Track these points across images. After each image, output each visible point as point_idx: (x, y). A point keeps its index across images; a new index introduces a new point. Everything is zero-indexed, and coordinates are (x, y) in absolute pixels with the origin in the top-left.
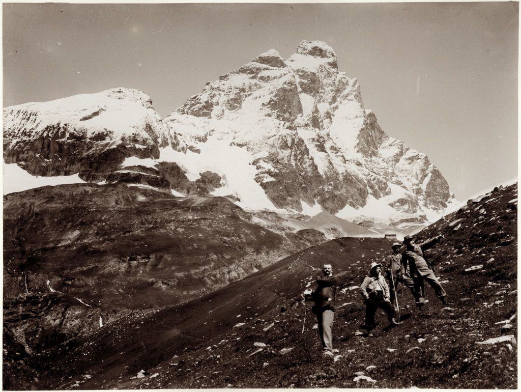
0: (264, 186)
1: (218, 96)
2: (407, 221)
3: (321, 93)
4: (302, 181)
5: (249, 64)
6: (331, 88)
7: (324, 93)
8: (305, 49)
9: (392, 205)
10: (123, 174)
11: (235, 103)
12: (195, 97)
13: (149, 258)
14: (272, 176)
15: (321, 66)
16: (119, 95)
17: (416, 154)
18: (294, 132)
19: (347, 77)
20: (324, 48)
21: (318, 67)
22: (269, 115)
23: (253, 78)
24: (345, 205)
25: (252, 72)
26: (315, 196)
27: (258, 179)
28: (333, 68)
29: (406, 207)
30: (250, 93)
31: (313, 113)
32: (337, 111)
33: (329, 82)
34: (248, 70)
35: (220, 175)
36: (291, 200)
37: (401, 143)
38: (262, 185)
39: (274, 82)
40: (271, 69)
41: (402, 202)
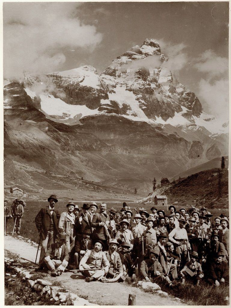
0: (143, 110)
2: (192, 125)
4: (155, 107)
8: (147, 43)
14: (145, 106)
15: (154, 51)
16: (86, 69)
17: (190, 92)
18: (150, 87)
20: (156, 42)
21: (153, 52)
22: (139, 78)
23: (129, 58)
25: (129, 56)
26: (159, 114)
27: (140, 107)
28: (159, 52)
38: (142, 109)
40: (137, 55)
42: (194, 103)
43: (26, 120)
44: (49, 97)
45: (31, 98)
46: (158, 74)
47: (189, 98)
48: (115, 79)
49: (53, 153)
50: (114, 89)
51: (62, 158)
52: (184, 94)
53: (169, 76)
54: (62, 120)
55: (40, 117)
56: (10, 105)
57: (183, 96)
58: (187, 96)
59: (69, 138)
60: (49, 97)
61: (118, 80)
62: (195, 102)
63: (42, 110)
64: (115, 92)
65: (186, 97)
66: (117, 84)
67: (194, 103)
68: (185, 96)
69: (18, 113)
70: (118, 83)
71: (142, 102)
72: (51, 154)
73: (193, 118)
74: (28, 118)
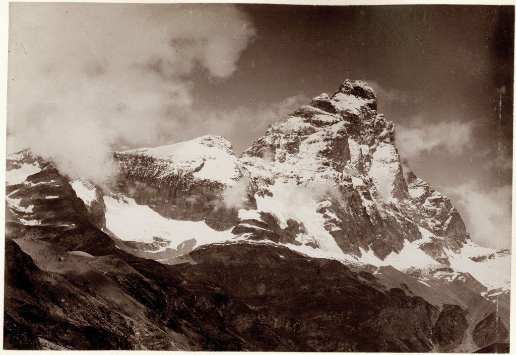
1: (279, 139)
2: (441, 270)
3: (362, 134)
4: (359, 230)
5: (304, 107)
6: (370, 130)
7: (364, 135)
8: (347, 88)
10: (246, 227)
11: (292, 148)
12: (261, 140)
13: (341, 313)
14: (337, 225)
15: (362, 107)
16: (210, 143)
17: (440, 197)
18: (350, 184)
19: (384, 119)
20: (366, 88)
22: (327, 164)
23: (307, 121)
25: (306, 116)
26: (369, 243)
27: (327, 228)
30: (305, 136)
31: (359, 160)
32: (375, 153)
33: (369, 123)
34: (303, 113)
35: (299, 222)
36: (353, 247)
37: (428, 185)
38: (331, 233)
39: (327, 128)
40: (323, 114)
42: (448, 221)
43: (71, 250)
44: (125, 202)
45: (86, 203)
46: (369, 158)
47: (438, 209)
49: (128, 324)
50: (271, 188)
51: (147, 335)
52: (427, 202)
53: (392, 161)
54: (153, 252)
55: (102, 243)
56: (38, 218)
57: (424, 205)
58: (433, 205)
59: (165, 291)
60: (125, 202)
61: (279, 167)
62: (450, 218)
63: (107, 230)
64: (271, 195)
65: (430, 208)
66: (277, 176)
67: (448, 221)
68: (429, 206)
69: (55, 236)
71: (330, 217)
72: (124, 325)
73: (445, 254)
74: (77, 247)
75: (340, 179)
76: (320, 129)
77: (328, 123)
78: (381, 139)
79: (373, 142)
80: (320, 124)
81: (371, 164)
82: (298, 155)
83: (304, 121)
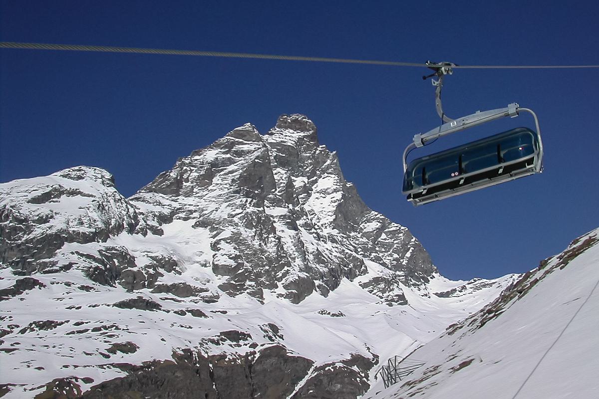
9: (364, 286)
18: (261, 209)
24: (312, 291)
25: (225, 147)
29: (382, 286)
41: (377, 281)
42: (408, 255)
48: (175, 201)
52: (384, 236)
53: (335, 191)
62: (411, 251)
65: (387, 241)
67: (408, 255)
68: (385, 239)
70: (180, 209)
75: (248, 205)
76: (240, 159)
77: (249, 152)
78: (323, 172)
79: (313, 173)
80: (240, 154)
81: (309, 195)
82: (210, 188)
83: (224, 153)
